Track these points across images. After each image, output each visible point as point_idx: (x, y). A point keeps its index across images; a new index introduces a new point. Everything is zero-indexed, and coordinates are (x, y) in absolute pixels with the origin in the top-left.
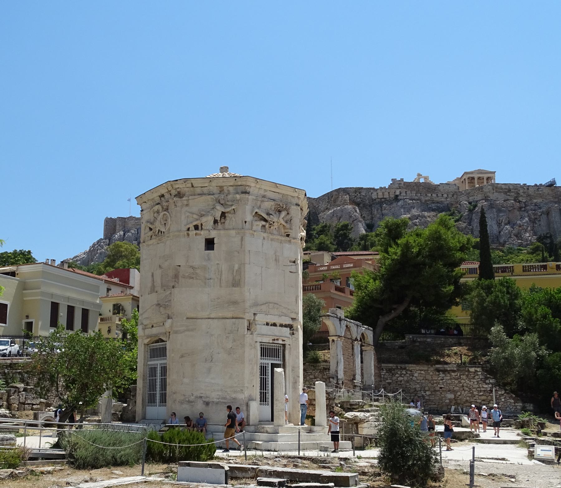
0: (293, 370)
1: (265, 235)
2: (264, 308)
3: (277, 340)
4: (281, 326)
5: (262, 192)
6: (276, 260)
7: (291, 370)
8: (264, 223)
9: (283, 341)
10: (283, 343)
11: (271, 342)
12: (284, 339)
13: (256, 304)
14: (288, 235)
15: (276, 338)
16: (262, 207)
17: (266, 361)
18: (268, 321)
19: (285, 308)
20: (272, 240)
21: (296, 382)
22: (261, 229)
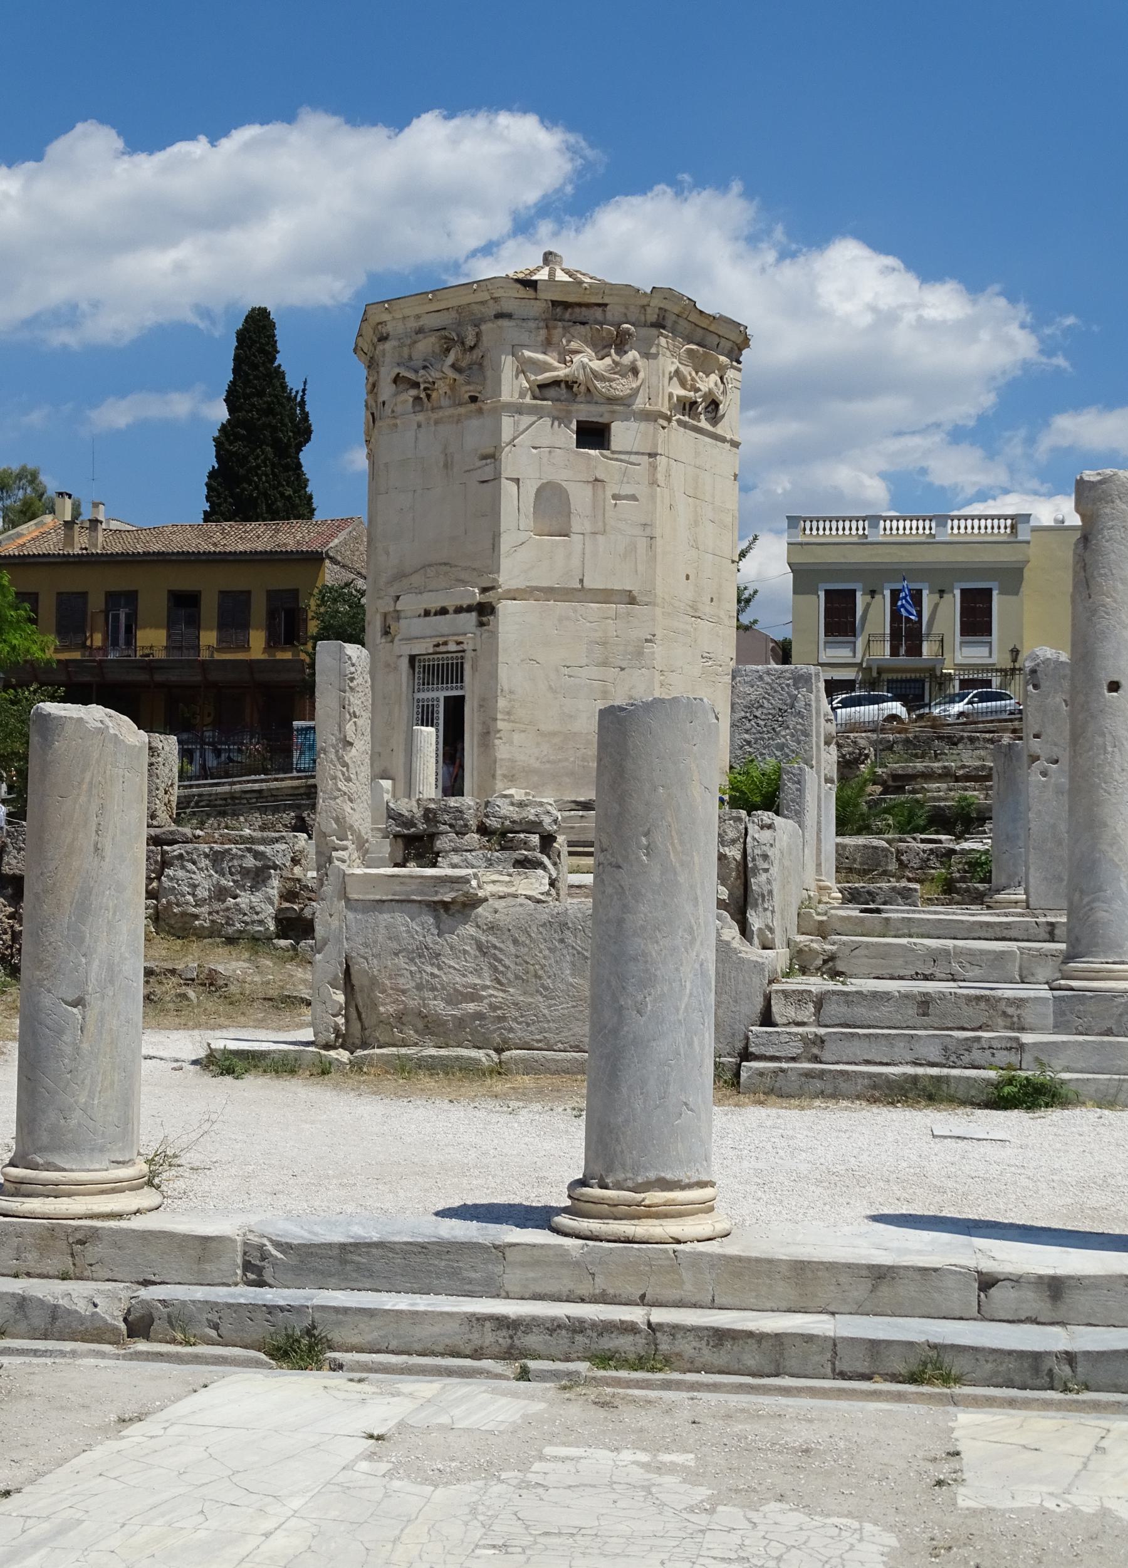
0: (481, 706)
1: (420, 417)
2: (416, 580)
3: (445, 643)
4: (459, 610)
5: (413, 324)
6: (446, 466)
7: (476, 705)
8: (414, 392)
9: (459, 643)
10: (459, 648)
11: (431, 651)
12: (460, 638)
13: (400, 576)
14: (473, 399)
15: (441, 640)
16: (414, 358)
17: (434, 694)
18: (428, 606)
19: (465, 569)
20: (436, 423)
21: (488, 733)
22: (413, 406)
